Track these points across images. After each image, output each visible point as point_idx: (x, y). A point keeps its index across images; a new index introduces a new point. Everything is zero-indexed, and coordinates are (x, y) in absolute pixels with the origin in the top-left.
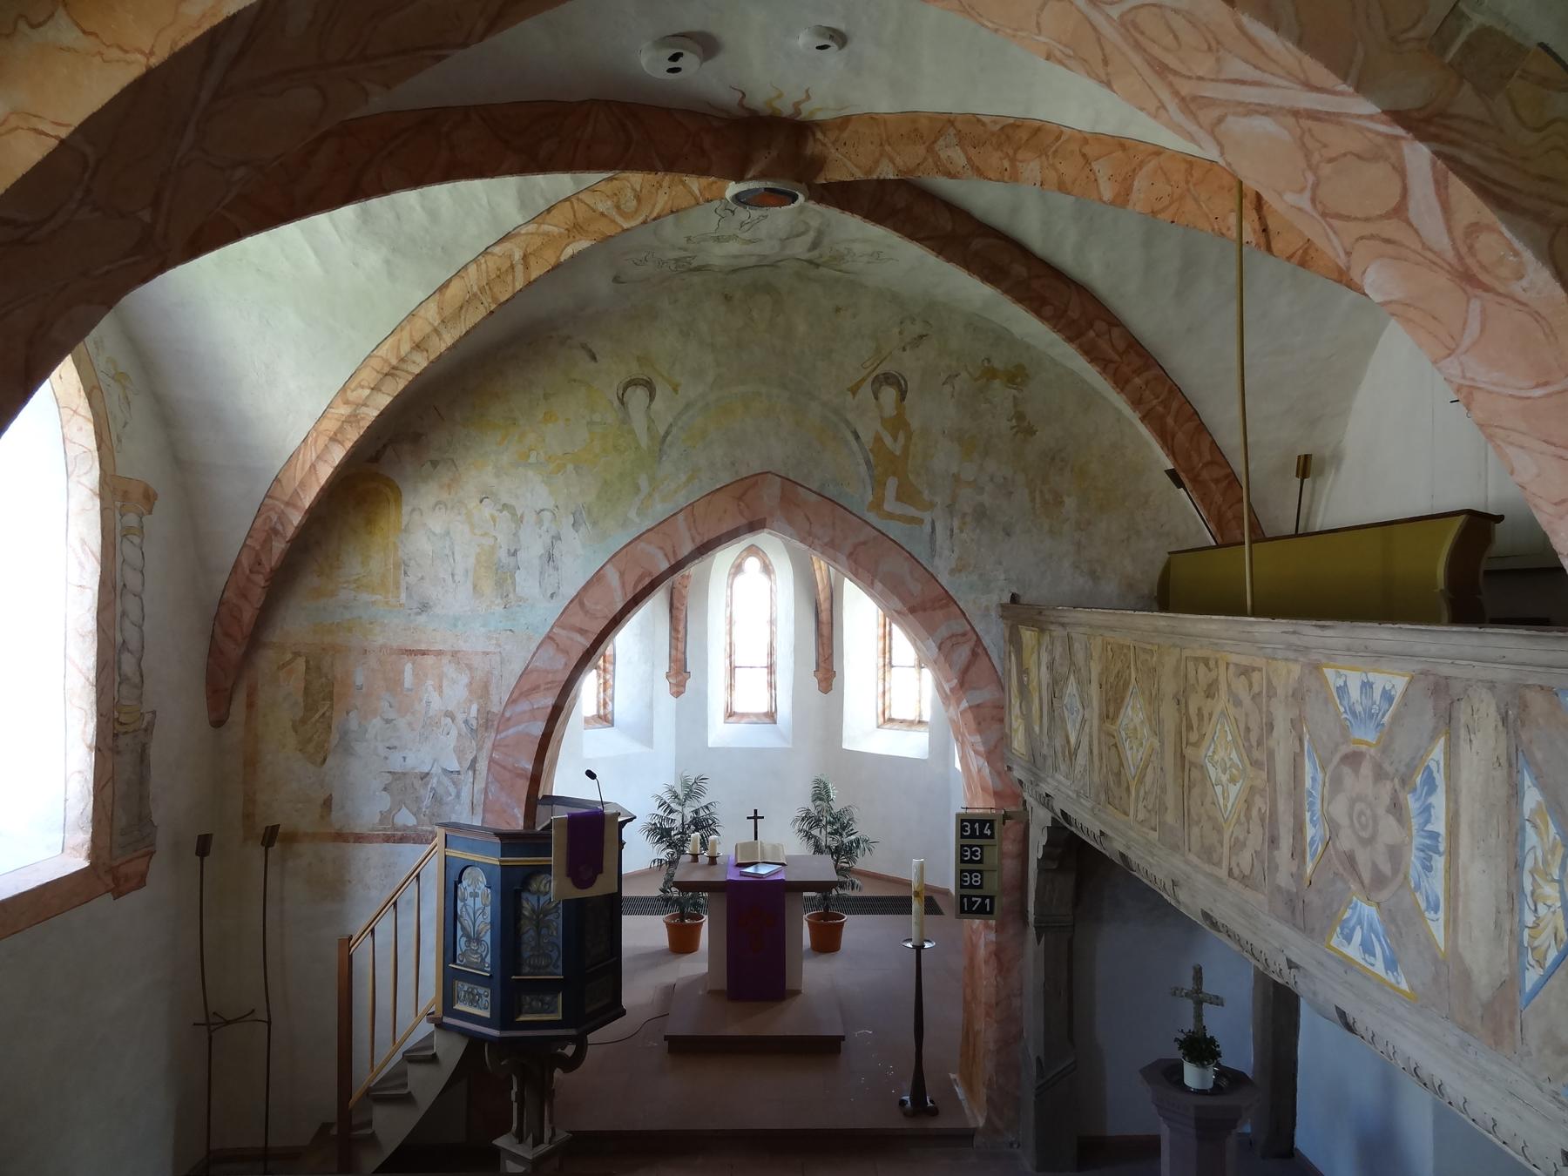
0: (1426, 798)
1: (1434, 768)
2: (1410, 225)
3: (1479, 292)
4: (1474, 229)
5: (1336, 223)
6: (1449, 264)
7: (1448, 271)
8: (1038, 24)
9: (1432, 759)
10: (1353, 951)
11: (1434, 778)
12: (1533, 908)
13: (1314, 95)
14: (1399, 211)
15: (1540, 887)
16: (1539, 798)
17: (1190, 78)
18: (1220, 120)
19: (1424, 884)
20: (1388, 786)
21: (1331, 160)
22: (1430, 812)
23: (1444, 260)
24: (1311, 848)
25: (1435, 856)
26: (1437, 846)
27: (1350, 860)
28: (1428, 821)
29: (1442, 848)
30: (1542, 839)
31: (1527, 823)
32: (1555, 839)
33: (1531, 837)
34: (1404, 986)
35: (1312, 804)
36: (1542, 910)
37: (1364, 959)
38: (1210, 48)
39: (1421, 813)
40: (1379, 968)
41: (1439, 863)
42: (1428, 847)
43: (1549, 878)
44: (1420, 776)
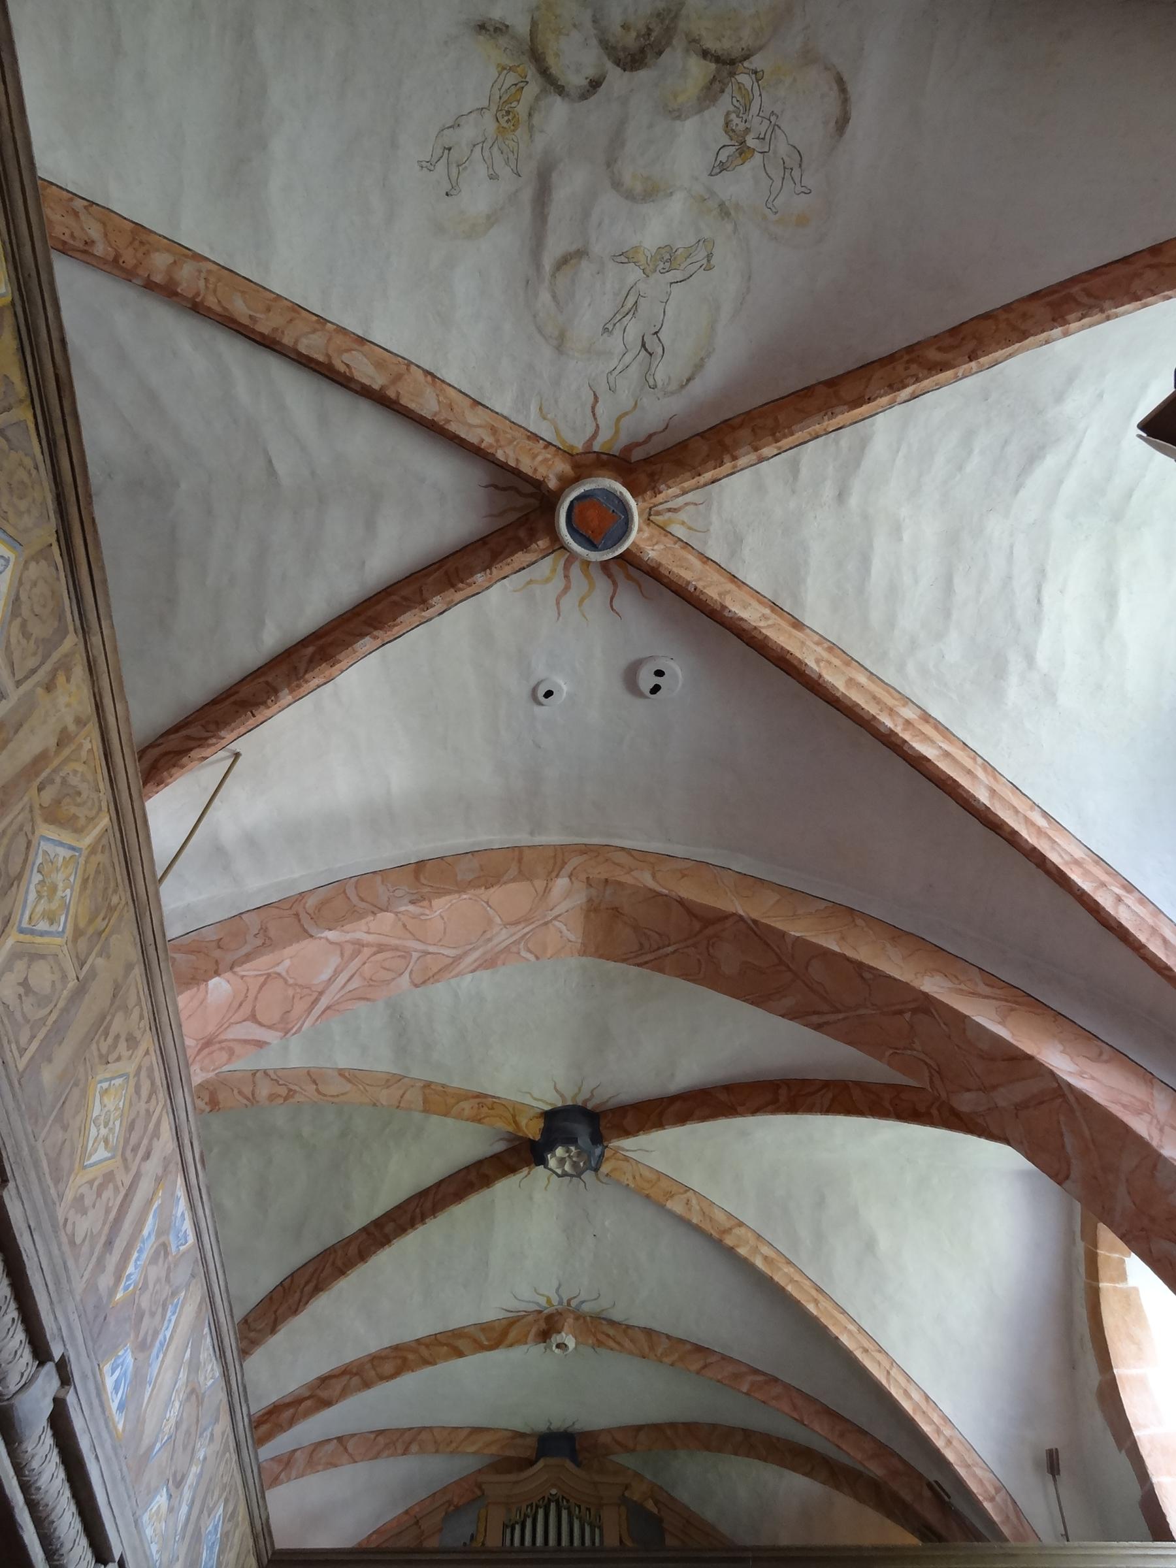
2: (244, 1021)
3: (199, 1047)
4: (231, 1052)
5: (262, 979)
6: (218, 1035)
7: (214, 1033)
8: (443, 919)
10: (109, 1382)
13: (324, 1007)
14: (253, 1018)
17: (369, 958)
18: (342, 955)
21: (293, 997)
23: (222, 1032)
24: (127, 1281)
27: (140, 1316)
34: (120, 1427)
35: (140, 1251)
37: (112, 1393)
38: (371, 979)
40: (114, 1406)
41: (161, 1356)
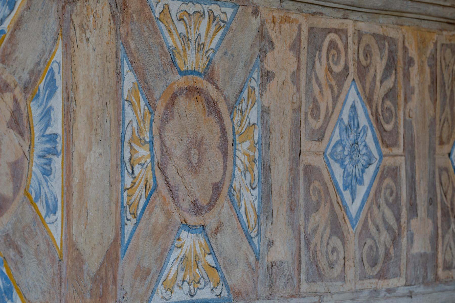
0: (47, 102)
1: (56, 70)
9: (56, 61)
11: (55, 80)
12: (130, 171)
15: (136, 152)
16: (134, 80)
19: (45, 190)
20: (8, 97)
22: (50, 115)
25: (55, 158)
26: (55, 148)
28: (47, 125)
29: (59, 148)
30: (136, 112)
31: (126, 102)
32: (144, 110)
33: (129, 114)
36: (137, 169)
39: (40, 121)
42: (48, 151)
43: (143, 142)
44: (44, 81)
